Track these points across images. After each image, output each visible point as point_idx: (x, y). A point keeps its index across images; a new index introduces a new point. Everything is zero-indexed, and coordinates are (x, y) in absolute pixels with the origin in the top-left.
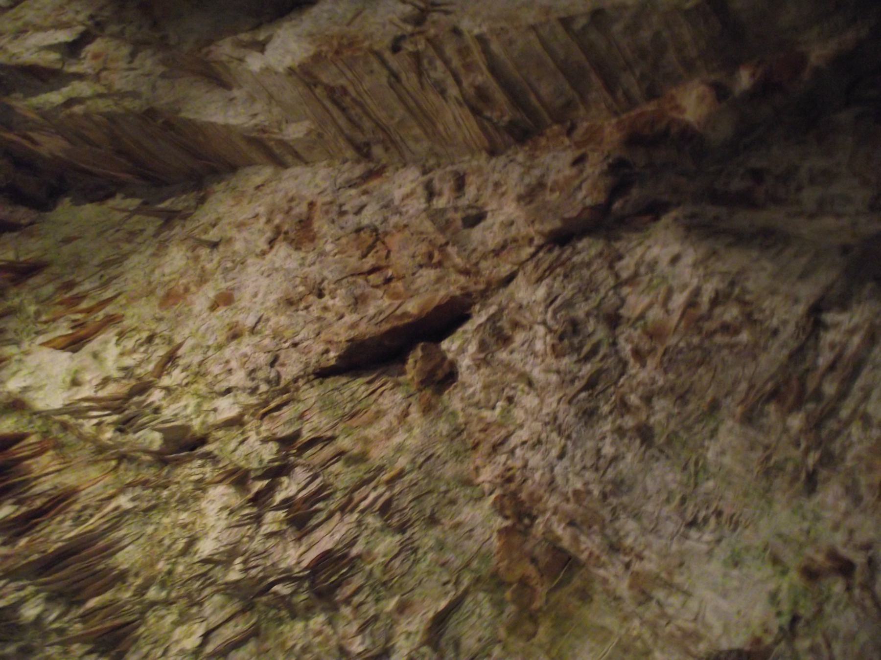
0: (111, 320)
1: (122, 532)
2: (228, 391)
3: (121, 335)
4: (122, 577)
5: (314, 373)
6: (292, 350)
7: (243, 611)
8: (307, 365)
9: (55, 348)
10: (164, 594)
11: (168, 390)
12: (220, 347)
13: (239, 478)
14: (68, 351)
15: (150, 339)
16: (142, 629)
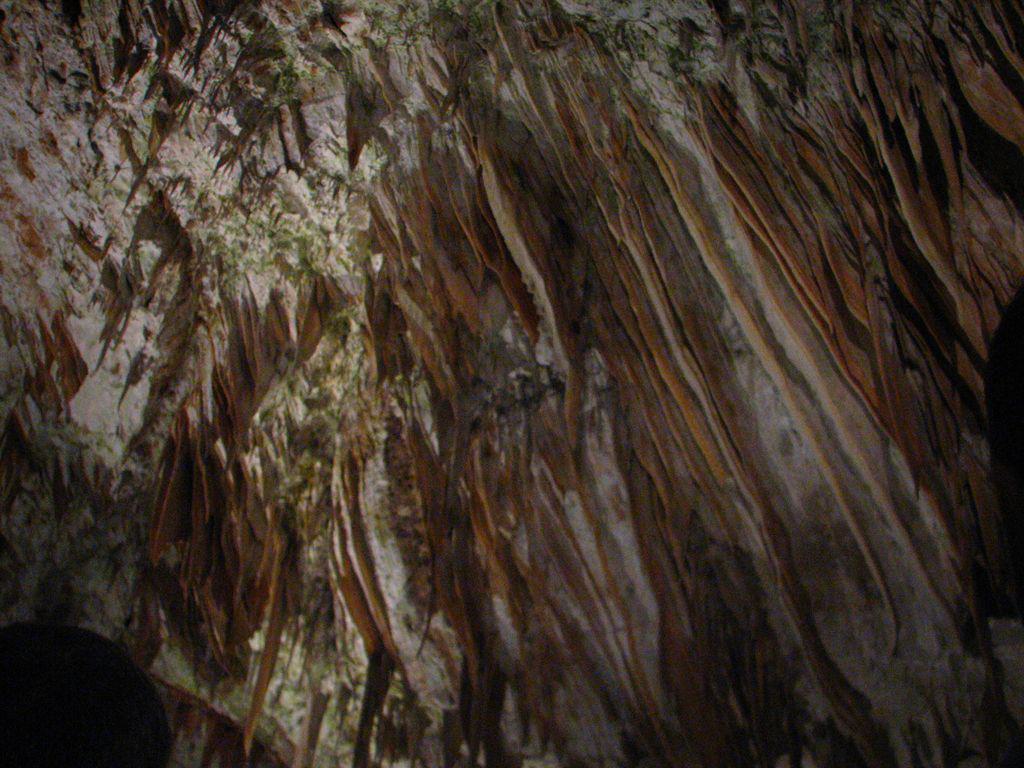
0: (58, 324)
1: (241, 301)
2: (94, 146)
3: (70, 308)
4: (275, 297)
5: (71, 25)
6: (45, 52)
7: (281, 122)
8: (61, 32)
9: (76, 390)
10: (294, 245)
11: (110, 240)
12: (64, 165)
13: (164, 124)
14: (83, 379)
15: (68, 267)
16: (325, 274)
